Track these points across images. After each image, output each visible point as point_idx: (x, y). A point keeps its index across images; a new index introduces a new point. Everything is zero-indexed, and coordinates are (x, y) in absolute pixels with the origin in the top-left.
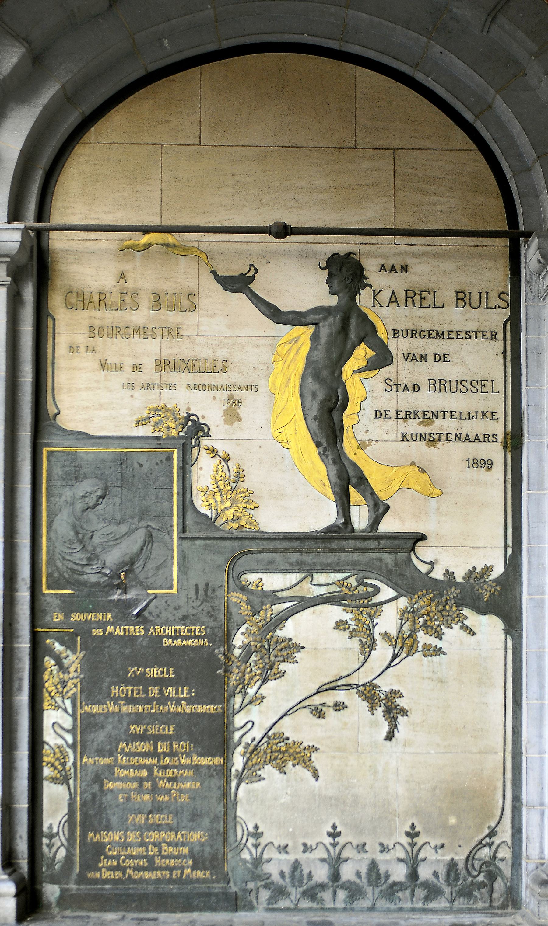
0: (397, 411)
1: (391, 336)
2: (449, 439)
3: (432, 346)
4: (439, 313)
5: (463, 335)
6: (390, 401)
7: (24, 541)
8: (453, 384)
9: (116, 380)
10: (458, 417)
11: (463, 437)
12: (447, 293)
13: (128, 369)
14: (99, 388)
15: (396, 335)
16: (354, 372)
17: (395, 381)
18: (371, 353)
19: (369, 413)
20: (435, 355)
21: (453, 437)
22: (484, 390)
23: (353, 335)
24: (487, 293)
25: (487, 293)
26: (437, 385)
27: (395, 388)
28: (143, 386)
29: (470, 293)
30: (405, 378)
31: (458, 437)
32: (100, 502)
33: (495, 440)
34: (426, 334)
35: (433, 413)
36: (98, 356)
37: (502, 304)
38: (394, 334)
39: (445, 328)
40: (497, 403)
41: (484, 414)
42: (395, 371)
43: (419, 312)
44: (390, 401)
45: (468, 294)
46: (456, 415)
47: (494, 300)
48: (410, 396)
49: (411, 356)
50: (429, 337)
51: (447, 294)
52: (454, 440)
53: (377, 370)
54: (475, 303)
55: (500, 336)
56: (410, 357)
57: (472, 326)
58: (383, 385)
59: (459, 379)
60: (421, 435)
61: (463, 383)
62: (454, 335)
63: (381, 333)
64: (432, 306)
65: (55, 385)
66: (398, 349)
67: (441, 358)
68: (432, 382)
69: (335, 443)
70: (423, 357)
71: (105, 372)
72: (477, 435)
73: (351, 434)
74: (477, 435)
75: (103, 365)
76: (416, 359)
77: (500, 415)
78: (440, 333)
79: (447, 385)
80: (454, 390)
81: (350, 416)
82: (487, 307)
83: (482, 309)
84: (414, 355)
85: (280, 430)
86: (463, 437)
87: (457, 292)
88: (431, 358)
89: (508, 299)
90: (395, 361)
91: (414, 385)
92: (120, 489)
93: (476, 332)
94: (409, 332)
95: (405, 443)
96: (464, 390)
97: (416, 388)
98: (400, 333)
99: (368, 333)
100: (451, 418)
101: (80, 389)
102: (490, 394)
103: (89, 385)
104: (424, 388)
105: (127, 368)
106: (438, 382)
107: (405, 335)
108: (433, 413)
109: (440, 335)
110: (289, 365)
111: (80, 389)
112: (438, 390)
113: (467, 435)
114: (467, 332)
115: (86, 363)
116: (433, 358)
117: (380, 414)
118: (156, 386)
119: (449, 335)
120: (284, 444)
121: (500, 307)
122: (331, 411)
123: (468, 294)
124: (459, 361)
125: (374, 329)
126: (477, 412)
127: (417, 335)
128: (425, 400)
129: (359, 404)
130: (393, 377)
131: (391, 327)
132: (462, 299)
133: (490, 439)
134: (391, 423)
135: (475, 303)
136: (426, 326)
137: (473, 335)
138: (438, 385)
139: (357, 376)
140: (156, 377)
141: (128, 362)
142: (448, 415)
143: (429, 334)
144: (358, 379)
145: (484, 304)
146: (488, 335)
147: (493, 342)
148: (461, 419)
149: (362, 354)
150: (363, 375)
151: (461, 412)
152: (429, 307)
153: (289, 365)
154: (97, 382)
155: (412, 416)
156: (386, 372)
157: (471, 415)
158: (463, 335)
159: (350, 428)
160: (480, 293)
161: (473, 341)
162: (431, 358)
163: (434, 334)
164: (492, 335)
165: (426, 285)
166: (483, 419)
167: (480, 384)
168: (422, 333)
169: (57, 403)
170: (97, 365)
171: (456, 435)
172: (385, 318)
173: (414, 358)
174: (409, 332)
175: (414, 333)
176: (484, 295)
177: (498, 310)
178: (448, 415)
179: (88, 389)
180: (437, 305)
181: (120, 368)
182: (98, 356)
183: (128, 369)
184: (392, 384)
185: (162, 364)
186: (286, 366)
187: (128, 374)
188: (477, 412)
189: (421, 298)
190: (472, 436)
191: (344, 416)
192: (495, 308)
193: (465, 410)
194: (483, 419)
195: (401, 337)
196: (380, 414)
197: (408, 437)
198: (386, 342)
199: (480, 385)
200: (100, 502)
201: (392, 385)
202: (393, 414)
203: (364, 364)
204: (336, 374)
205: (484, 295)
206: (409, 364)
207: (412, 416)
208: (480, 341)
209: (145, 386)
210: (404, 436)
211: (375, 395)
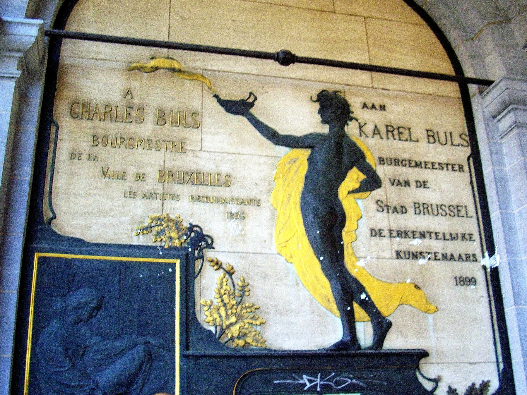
0: (390, 230)
1: (378, 163)
2: (437, 258)
3: (413, 174)
4: (415, 146)
5: (436, 166)
6: (383, 221)
7: (5, 356)
8: (434, 207)
9: (118, 188)
10: (442, 238)
11: (449, 256)
12: (420, 131)
13: (130, 177)
14: (99, 195)
15: (382, 162)
16: (350, 192)
17: (385, 202)
18: (362, 177)
19: (364, 231)
20: (417, 181)
21: (440, 256)
22: (461, 214)
23: (346, 159)
24: (451, 133)
25: (451, 133)
26: (421, 208)
27: (385, 209)
28: (145, 196)
29: (438, 132)
30: (394, 199)
31: (445, 257)
32: (94, 314)
33: (474, 259)
34: (407, 163)
35: (421, 234)
36: (100, 164)
37: (464, 143)
38: (380, 161)
39: (423, 159)
40: (471, 225)
41: (463, 236)
42: (384, 194)
43: (401, 144)
44: (383, 221)
45: (436, 133)
46: (440, 236)
47: (457, 140)
48: (399, 216)
49: (396, 181)
50: (410, 166)
51: (419, 132)
52: (441, 259)
53: (369, 193)
54: (443, 140)
55: (466, 168)
56: (395, 182)
57: (443, 159)
58: (374, 207)
59: (439, 204)
60: (413, 254)
61: (443, 207)
62: (429, 166)
63: (371, 160)
64: (409, 139)
65: (53, 190)
66: (385, 175)
67: (422, 184)
68: (417, 205)
69: (337, 260)
70: (407, 183)
71: (107, 179)
72: (460, 255)
73: (350, 251)
74: (460, 255)
75: (105, 173)
76: (401, 184)
77: (476, 236)
78: (418, 163)
79: (430, 208)
80: (436, 213)
81: (349, 233)
82: (452, 144)
83: (448, 146)
84: (399, 181)
85: (284, 244)
86: (449, 256)
87: (427, 131)
88: (413, 184)
89: (468, 139)
90: (383, 185)
91: (402, 207)
92: (117, 301)
93: (447, 165)
94: (393, 161)
95: (400, 261)
96: (444, 213)
97: (404, 210)
98: (385, 161)
99: (358, 159)
100: (437, 239)
101: (79, 195)
102: (465, 218)
103: (89, 192)
104: (411, 210)
105: (128, 176)
106: (421, 206)
107: (389, 162)
108: (421, 234)
109: (418, 165)
110: (289, 183)
111: (79, 195)
112: (422, 212)
113: (452, 255)
114: (440, 164)
115: (85, 167)
116: (414, 184)
117: (376, 233)
118: (159, 196)
119: (426, 165)
120: (288, 258)
121: (462, 145)
122: (331, 227)
123: (436, 133)
124: (437, 188)
125: (362, 156)
126: (457, 234)
127: (400, 163)
128: (412, 221)
129: (355, 222)
130: (383, 198)
131: (377, 155)
132: (433, 136)
133: (471, 258)
134: (386, 241)
135: (443, 140)
136: (406, 156)
137: (445, 166)
138: (422, 208)
139: (352, 196)
140: (159, 188)
141: (132, 171)
142: (433, 235)
143: (410, 164)
144: (353, 200)
145: (449, 142)
146: (457, 168)
147: (461, 174)
148: (444, 239)
149: (354, 178)
150: (358, 195)
151: (444, 234)
152: (407, 140)
153: (289, 183)
154: (98, 188)
155: (403, 235)
156: (378, 193)
157: (453, 237)
158: (436, 166)
159: (349, 245)
160: (445, 133)
161: (444, 172)
162: (413, 184)
163: (413, 164)
164: (460, 168)
165: (402, 123)
166: (463, 240)
167: (456, 209)
168: (404, 163)
169: (54, 208)
170: (98, 172)
171: (443, 255)
172: (372, 148)
173: (399, 184)
174: (393, 161)
175: (397, 162)
176: (448, 135)
177: (460, 148)
178: (433, 235)
179: (87, 195)
180: (413, 139)
181: (122, 176)
182: (100, 164)
183: (130, 177)
184: (383, 206)
185: (166, 175)
186: (286, 184)
187: (129, 184)
188: (457, 234)
189: (400, 133)
190: (456, 256)
191: (343, 233)
192: (459, 145)
193: (447, 232)
194: (463, 240)
195: (386, 164)
196: (376, 233)
197: (402, 254)
198: (374, 167)
199: (455, 210)
200: (94, 314)
201: (384, 207)
202: (386, 233)
203: (357, 186)
204: (334, 193)
205: (448, 135)
206: (394, 188)
207: (403, 235)
208: (450, 171)
209: (148, 195)
210: (398, 253)
211: (369, 214)
